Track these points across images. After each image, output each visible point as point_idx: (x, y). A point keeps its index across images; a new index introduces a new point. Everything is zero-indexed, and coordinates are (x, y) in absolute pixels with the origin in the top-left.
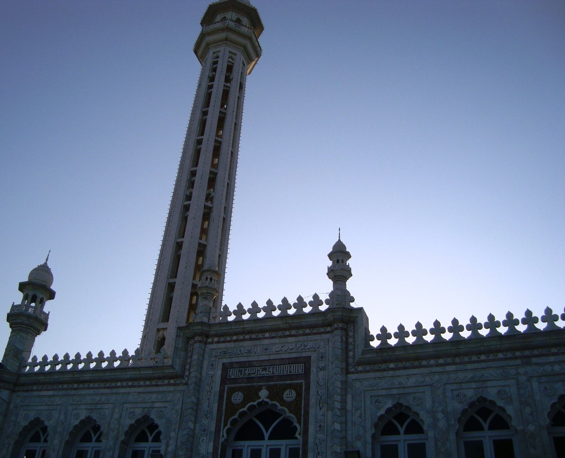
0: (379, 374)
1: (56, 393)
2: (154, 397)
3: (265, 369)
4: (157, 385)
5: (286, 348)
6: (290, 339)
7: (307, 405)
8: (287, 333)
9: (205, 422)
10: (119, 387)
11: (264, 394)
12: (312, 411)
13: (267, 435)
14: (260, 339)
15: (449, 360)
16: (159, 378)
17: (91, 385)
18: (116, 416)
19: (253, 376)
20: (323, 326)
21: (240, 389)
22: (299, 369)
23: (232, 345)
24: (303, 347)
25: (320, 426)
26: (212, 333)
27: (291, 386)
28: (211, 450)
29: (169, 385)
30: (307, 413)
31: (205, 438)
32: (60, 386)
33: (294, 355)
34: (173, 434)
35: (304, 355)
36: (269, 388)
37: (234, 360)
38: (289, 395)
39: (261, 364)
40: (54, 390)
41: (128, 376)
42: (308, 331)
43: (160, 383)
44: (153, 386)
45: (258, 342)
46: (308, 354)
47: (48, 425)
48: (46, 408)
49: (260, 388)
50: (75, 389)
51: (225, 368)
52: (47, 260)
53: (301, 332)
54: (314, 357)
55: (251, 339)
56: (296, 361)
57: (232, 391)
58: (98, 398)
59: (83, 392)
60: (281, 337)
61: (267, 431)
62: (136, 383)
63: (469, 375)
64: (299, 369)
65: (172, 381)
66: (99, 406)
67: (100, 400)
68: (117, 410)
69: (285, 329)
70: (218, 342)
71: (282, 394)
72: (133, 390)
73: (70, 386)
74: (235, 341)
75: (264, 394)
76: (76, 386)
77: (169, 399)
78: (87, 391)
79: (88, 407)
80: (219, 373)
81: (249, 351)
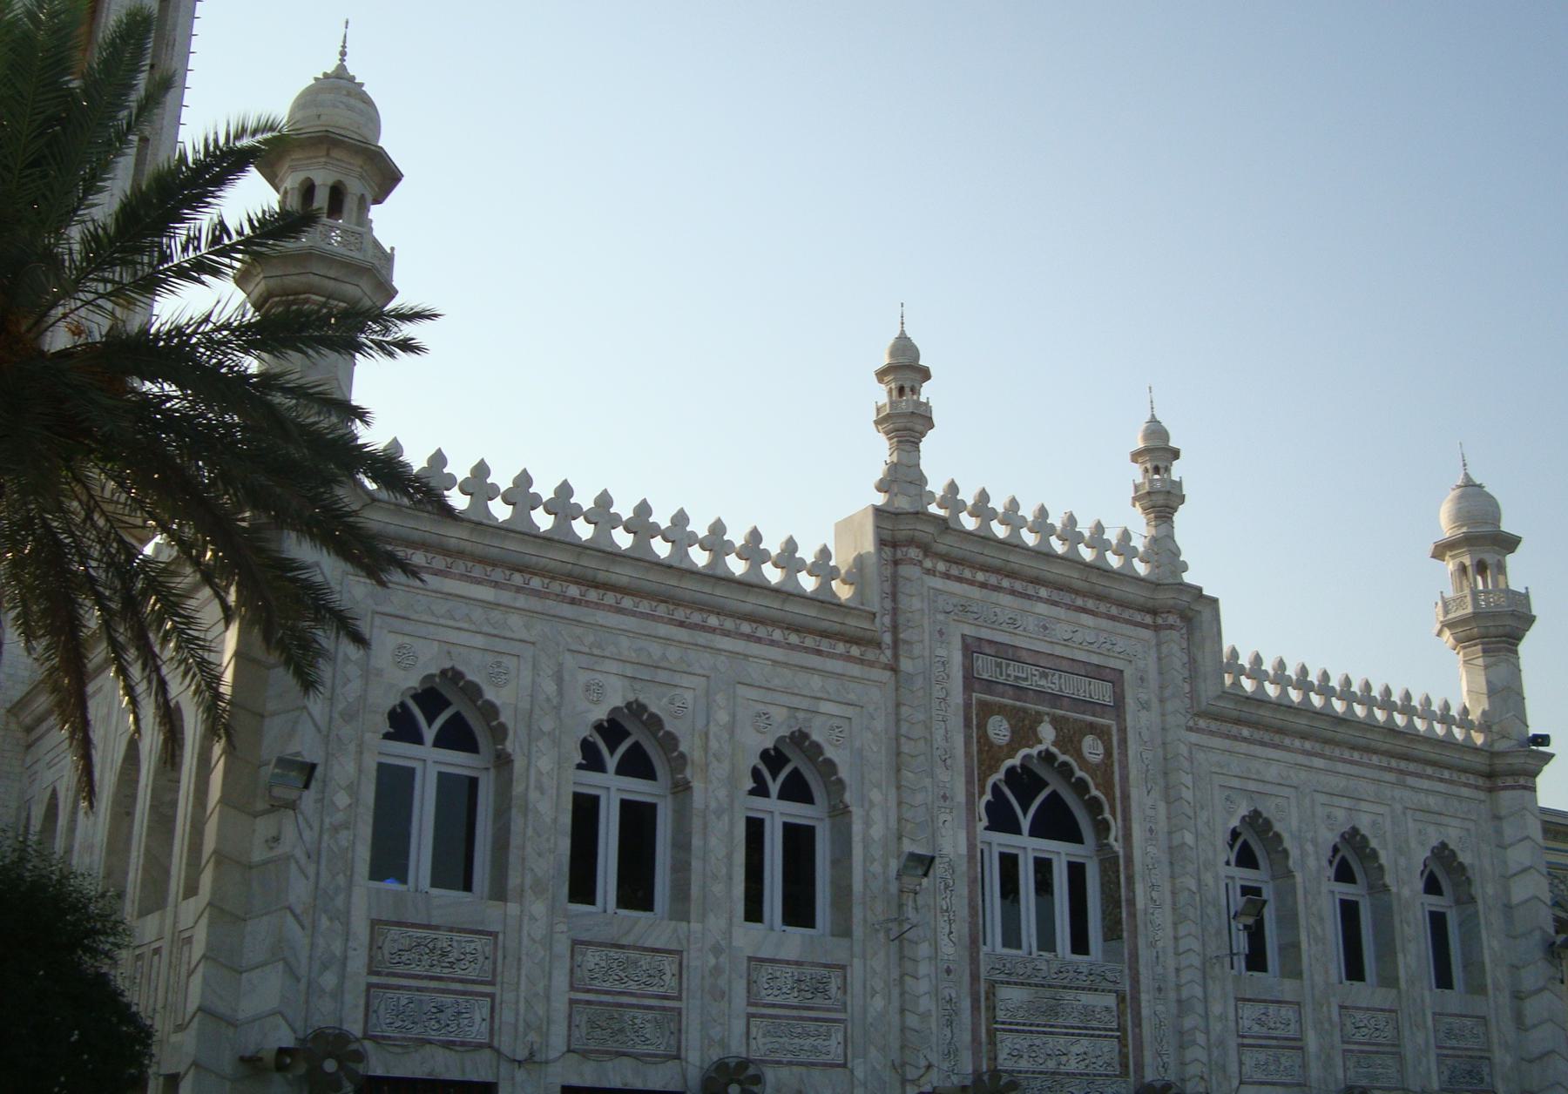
0: (1227, 743)
1: (505, 597)
2: (816, 682)
3: (1044, 675)
4: (819, 652)
5: (1078, 637)
6: (1086, 619)
7: (1125, 778)
8: (1079, 602)
9: (943, 775)
10: (713, 630)
11: (1047, 732)
12: (1134, 793)
13: (1025, 824)
14: (1029, 597)
15: (1318, 747)
16: (824, 634)
17: (627, 602)
18: (723, 717)
19: (1024, 684)
20: (1143, 609)
21: (1002, 710)
22: (1101, 692)
23: (975, 592)
24: (1108, 646)
25: (1151, 830)
26: (942, 548)
27: (1092, 728)
28: (963, 849)
29: (848, 658)
30: (1126, 797)
31: (949, 818)
32: (518, 579)
33: (1095, 659)
34: (876, 796)
35: (1112, 663)
36: (1056, 722)
37: (986, 634)
38: (1092, 748)
39: (1036, 660)
40: (496, 585)
41: (747, 608)
42: (1114, 611)
43: (825, 645)
44: (807, 650)
45: (1026, 604)
46: (1118, 664)
47: (498, 702)
48: (479, 641)
49: (1038, 719)
50: (573, 601)
51: (971, 648)
52: (343, 54)
53: (1103, 608)
55: (1013, 592)
56: (1096, 672)
57: (987, 710)
58: (656, 650)
59: (602, 617)
60: (1069, 607)
61: (1025, 814)
62: (762, 632)
63: (1342, 783)
66: (662, 676)
67: (664, 657)
68: (720, 699)
69: (1077, 592)
70: (947, 576)
71: (1080, 742)
72: (755, 649)
73: (556, 587)
74: (983, 585)
75: (1047, 732)
76: (573, 591)
77: (852, 697)
78: (613, 620)
79: (629, 671)
80: (957, 658)
81: (1013, 621)
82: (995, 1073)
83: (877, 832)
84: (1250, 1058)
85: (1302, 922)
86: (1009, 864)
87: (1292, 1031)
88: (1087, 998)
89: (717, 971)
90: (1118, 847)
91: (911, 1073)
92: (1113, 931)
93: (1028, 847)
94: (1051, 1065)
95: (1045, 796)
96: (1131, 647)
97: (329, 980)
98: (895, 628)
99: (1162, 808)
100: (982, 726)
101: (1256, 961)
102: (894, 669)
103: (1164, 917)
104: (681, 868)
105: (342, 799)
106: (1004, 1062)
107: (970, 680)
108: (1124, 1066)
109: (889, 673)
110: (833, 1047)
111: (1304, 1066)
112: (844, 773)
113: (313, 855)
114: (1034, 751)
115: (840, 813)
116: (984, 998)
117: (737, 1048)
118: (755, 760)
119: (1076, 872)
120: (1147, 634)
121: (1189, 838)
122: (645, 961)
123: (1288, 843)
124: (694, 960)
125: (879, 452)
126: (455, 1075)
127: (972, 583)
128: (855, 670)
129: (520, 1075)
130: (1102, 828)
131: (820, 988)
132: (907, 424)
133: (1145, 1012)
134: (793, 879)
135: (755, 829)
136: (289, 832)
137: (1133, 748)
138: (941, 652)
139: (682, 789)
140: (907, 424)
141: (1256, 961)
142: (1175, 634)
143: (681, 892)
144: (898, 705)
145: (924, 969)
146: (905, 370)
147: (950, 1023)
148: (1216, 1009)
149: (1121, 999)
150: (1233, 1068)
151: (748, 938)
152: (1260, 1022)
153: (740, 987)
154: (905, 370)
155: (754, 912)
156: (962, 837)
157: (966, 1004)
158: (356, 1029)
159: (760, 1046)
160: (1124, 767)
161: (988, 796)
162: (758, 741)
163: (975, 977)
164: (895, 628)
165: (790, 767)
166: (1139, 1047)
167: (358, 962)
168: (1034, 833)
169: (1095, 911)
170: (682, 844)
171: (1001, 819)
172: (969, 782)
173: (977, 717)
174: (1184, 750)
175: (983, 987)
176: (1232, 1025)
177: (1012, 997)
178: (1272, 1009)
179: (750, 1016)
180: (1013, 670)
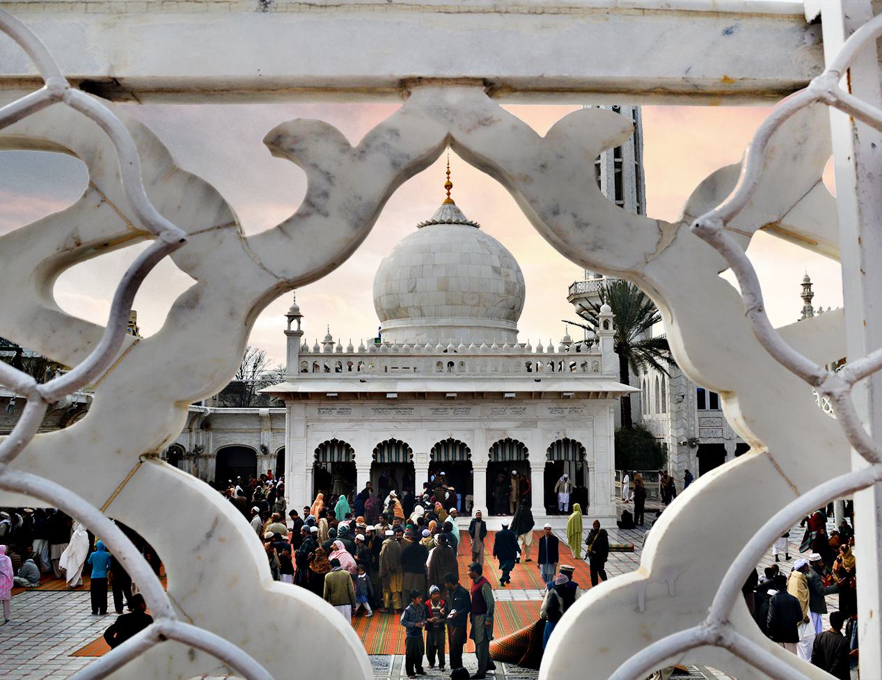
97: (692, 429)
105: (691, 397)
113: (687, 408)
125: (802, 303)
126: (716, 443)
129: (728, 441)
132: (808, 298)
136: (682, 405)
140: (808, 298)
146: (807, 285)
154: (807, 285)
158: (697, 436)
167: (697, 425)
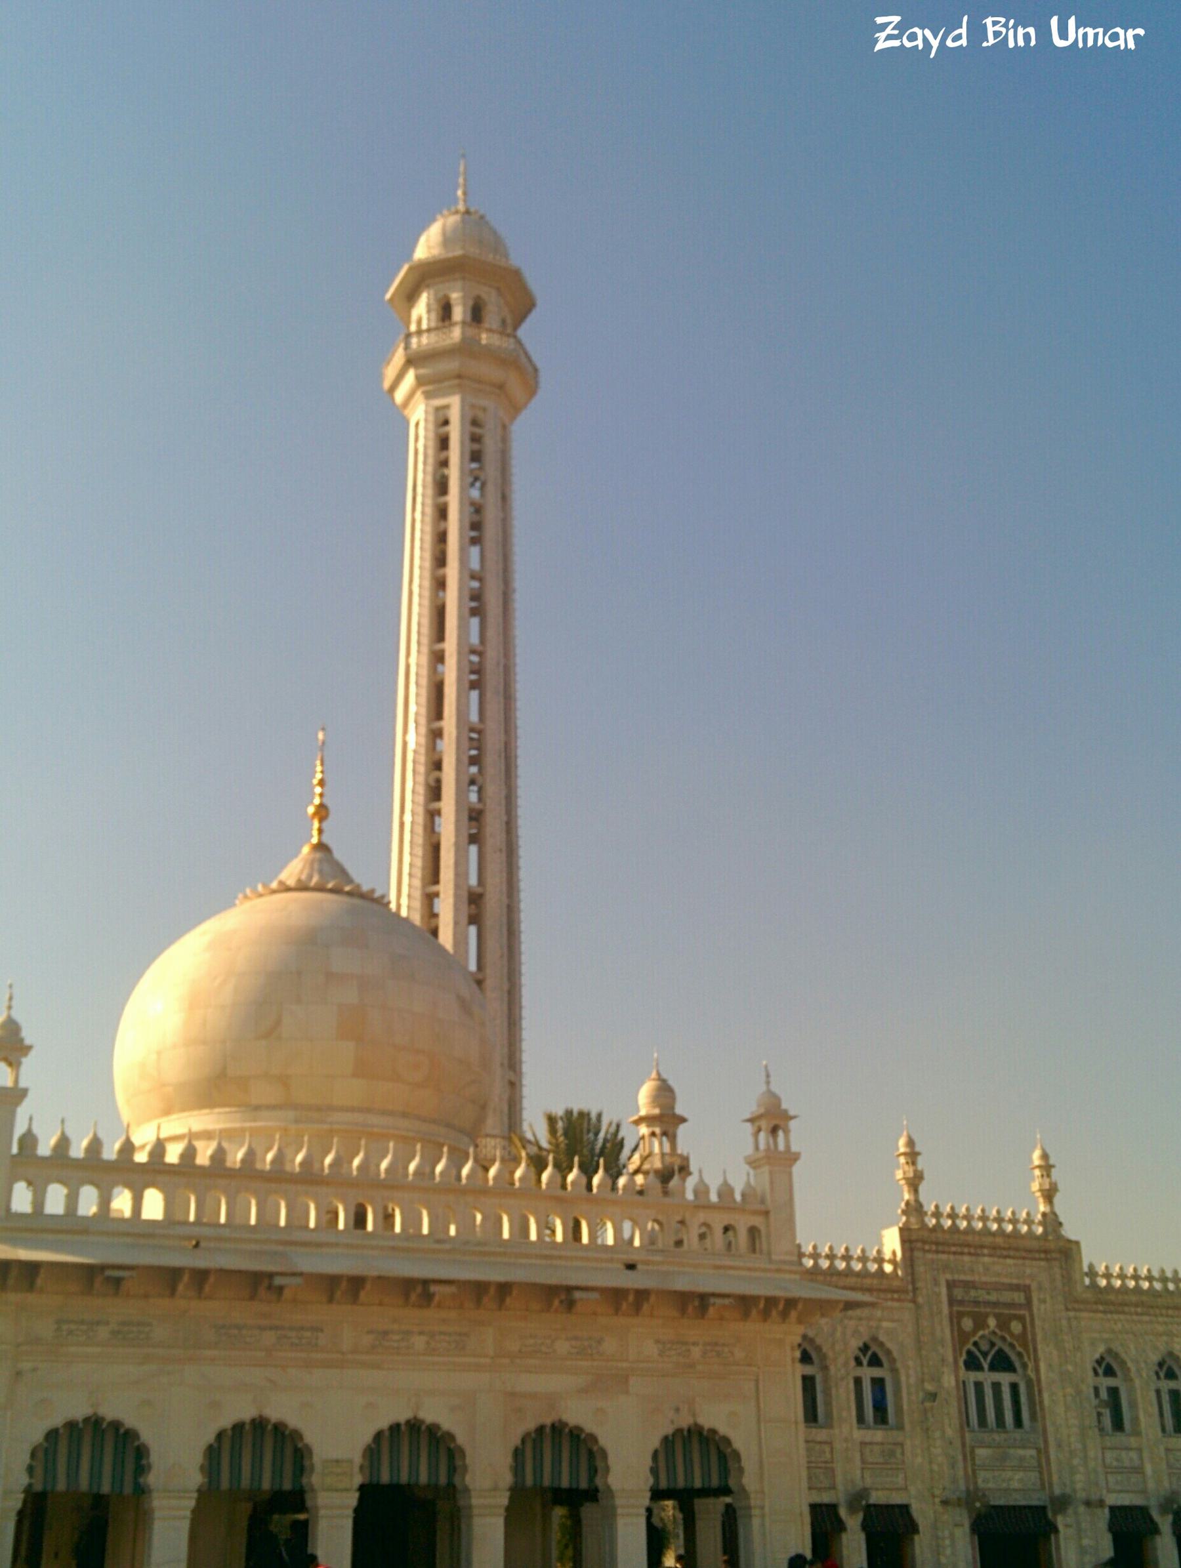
0: (1092, 1315)
3: (988, 1294)
6: (1009, 1261)
11: (992, 1322)
13: (986, 1366)
20: (1039, 1251)
21: (969, 1314)
22: (1019, 1297)
29: (893, 1300)
30: (1035, 1350)
33: (1015, 1281)
34: (911, 1363)
36: (997, 1316)
37: (956, 1277)
38: (1016, 1327)
39: (986, 1287)
46: (1027, 1282)
49: (987, 1315)
51: (951, 1285)
53: (1018, 1254)
54: (1034, 1286)
56: (1017, 1288)
57: (960, 1315)
64: (1019, 1297)
65: (896, 1296)
69: (1004, 1249)
70: (937, 1252)
75: (992, 1322)
80: (944, 1290)
82: (977, 1489)
83: (912, 1380)
84: (1111, 1479)
85: (1140, 1406)
86: (979, 1386)
87: (1137, 1462)
88: (1021, 1452)
89: (847, 1449)
90: (1033, 1375)
91: (937, 1492)
92: (1033, 1417)
93: (987, 1377)
94: (1004, 1485)
95: (995, 1354)
96: (1034, 1272)
98: (913, 1282)
99: (1055, 1352)
100: (959, 1323)
101: (1118, 1425)
102: (914, 1301)
103: (1060, 1410)
104: (828, 1404)
106: (981, 1484)
107: (952, 1301)
108: (1043, 1484)
109: (911, 1305)
110: (900, 1480)
111: (1145, 1482)
112: (895, 1354)
114: (986, 1332)
115: (894, 1371)
116: (969, 1455)
117: (860, 1484)
118: (857, 1352)
119: (1014, 1387)
120: (1043, 1263)
121: (1070, 1368)
122: (818, 1447)
123: (1130, 1364)
124: (838, 1446)
127: (949, 1253)
128: (896, 1304)
130: (1025, 1366)
131: (892, 1453)
133: (1052, 1457)
134: (879, 1408)
135: (858, 1381)
137: (1037, 1322)
138: (937, 1290)
139: (825, 1368)
141: (1118, 1425)
142: (1057, 1263)
143: (829, 1415)
144: (917, 1320)
145: (938, 1443)
147: (953, 1467)
148: (1091, 1454)
149: (1039, 1451)
150: (1103, 1483)
151: (858, 1434)
152: (1117, 1460)
153: (858, 1456)
155: (861, 1419)
156: (953, 1379)
157: (960, 1457)
159: (868, 1482)
160: (1034, 1334)
161: (964, 1356)
162: (855, 1344)
163: (964, 1445)
164: (913, 1282)
165: (871, 1355)
166: (1050, 1475)
168: (993, 1368)
169: (1018, 1412)
170: (827, 1393)
171: (972, 1364)
172: (954, 1350)
173: (955, 1319)
174: (1064, 1323)
175: (968, 1450)
176: (1100, 1461)
177: (981, 1452)
178: (1124, 1454)
179: (863, 1469)
180: (973, 1293)
